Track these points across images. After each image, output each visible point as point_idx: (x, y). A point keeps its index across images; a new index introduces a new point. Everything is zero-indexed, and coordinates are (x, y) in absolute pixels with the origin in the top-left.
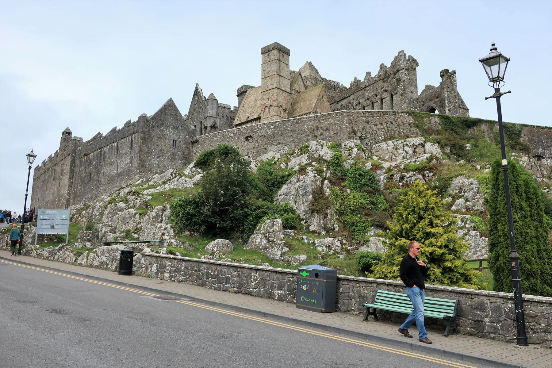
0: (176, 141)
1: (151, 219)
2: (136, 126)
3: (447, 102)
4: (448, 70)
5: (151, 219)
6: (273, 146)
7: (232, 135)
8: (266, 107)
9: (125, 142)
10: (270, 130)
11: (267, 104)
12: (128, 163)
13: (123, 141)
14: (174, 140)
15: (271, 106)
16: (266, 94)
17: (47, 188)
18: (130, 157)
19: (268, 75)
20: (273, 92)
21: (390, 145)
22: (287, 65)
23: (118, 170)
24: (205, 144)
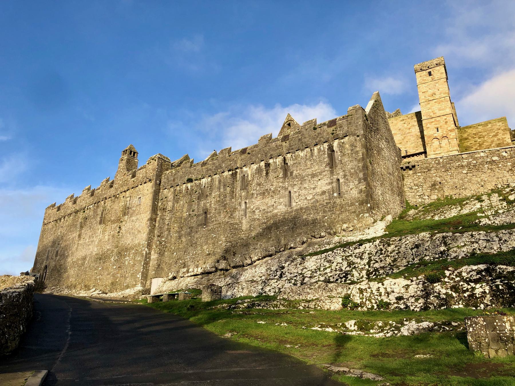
2: (341, 127)
9: (308, 155)
12: (324, 193)
13: (302, 154)
16: (432, 122)
17: (80, 236)
18: (329, 181)
19: (433, 99)
20: (445, 119)
23: (294, 204)
24: (432, 172)
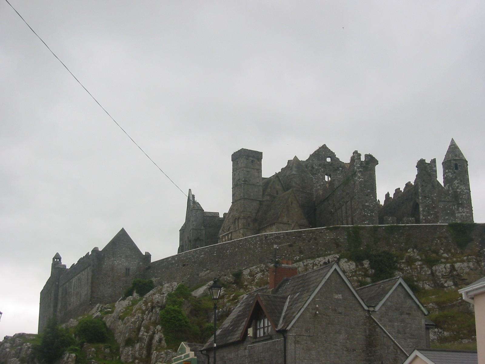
0: (129, 269)
1: (12, 355)
3: (420, 198)
4: (424, 160)
5: (12, 355)
6: (204, 271)
7: (173, 262)
8: (236, 219)
10: (201, 256)
11: (236, 216)
14: (126, 269)
15: (239, 218)
21: (301, 265)
22: (259, 170)
